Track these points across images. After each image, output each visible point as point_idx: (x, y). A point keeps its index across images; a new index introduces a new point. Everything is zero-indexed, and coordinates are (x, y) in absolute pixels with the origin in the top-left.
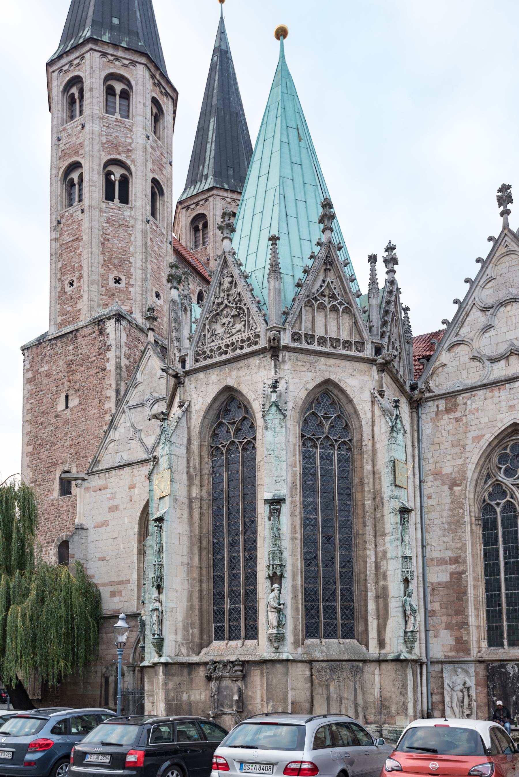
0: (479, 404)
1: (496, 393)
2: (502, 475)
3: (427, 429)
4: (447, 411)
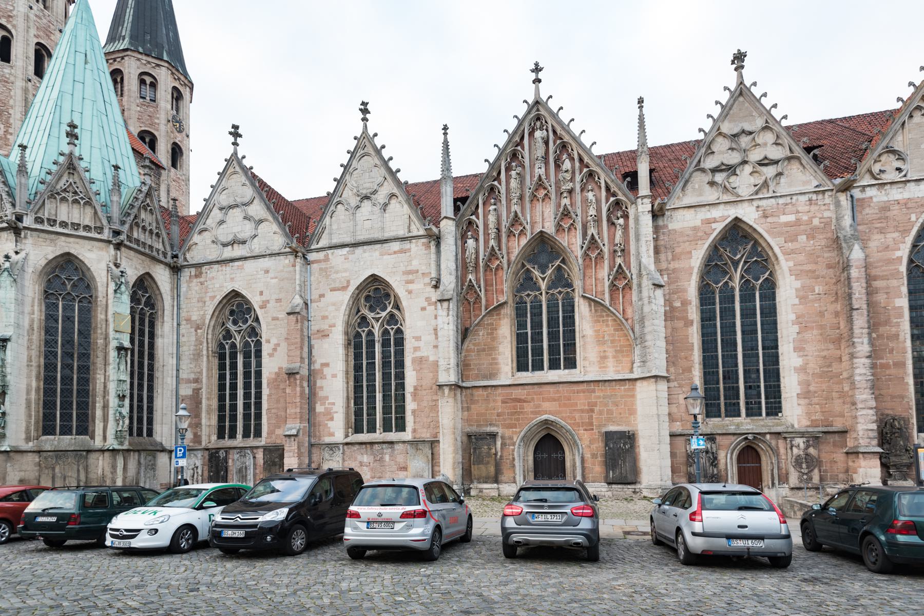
0: (214, 274)
1: (224, 268)
2: (230, 323)
3: (183, 289)
4: (196, 276)
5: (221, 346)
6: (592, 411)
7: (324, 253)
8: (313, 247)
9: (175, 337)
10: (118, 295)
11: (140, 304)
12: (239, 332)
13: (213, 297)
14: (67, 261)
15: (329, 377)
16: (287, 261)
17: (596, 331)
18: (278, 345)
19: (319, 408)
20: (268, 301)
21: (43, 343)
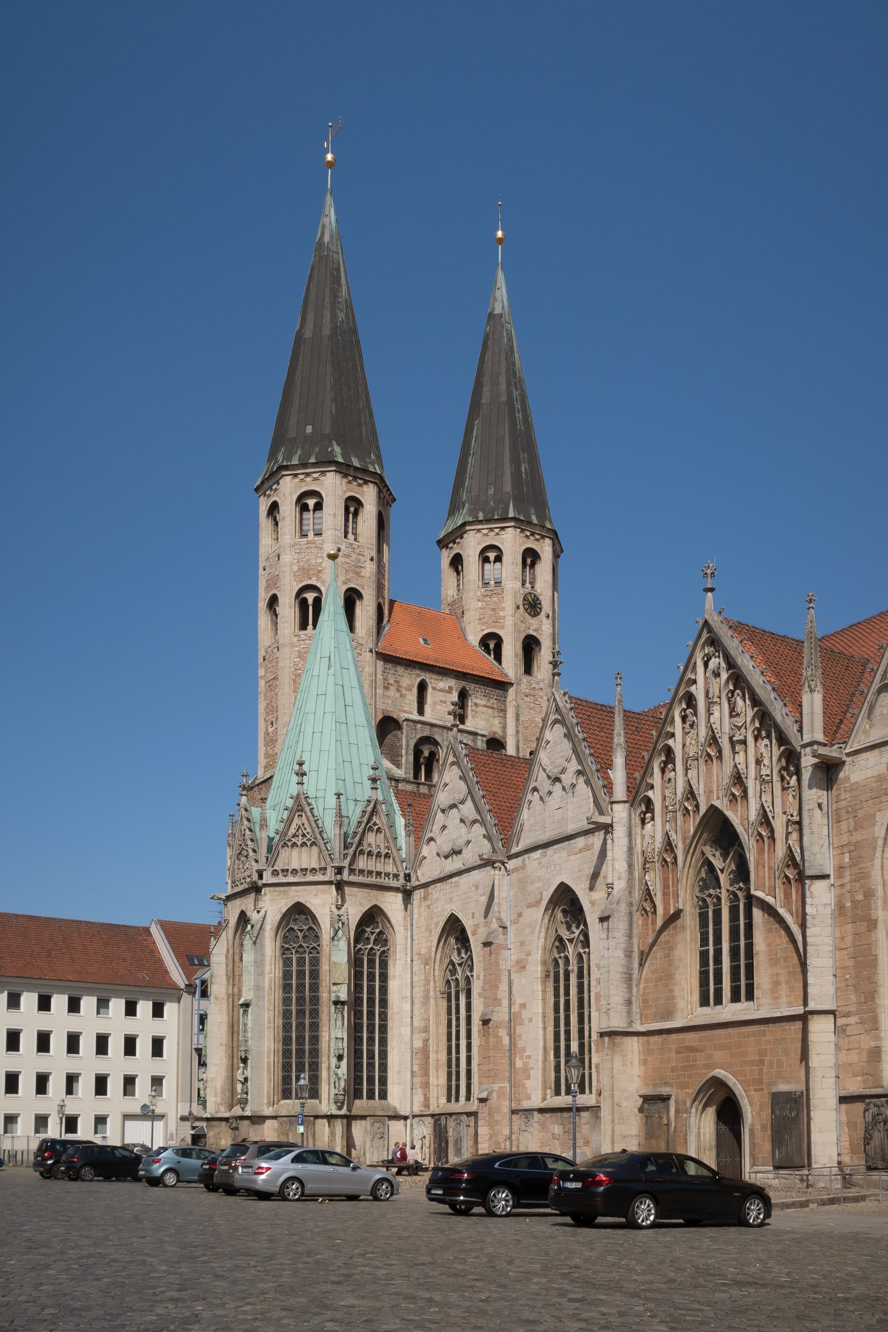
6: (762, 1062)
7: (520, 859)
9: (409, 976)
10: (336, 943)
11: (369, 944)
13: (437, 924)
14: (299, 910)
15: (526, 1022)
17: (769, 945)
19: (519, 1064)
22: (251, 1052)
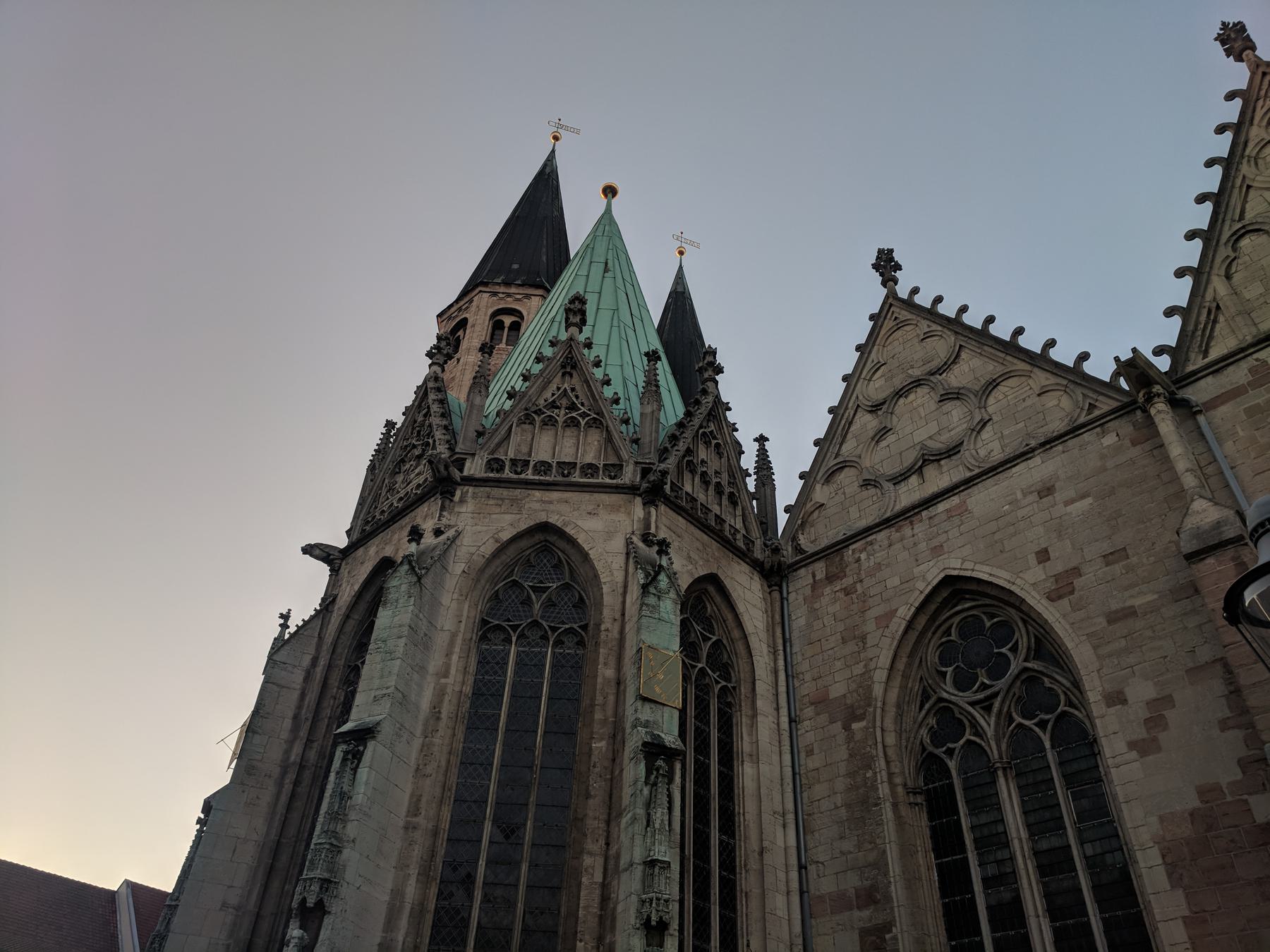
0: (880, 556)
1: (907, 531)
2: (949, 686)
3: (799, 620)
4: (830, 579)
5: (931, 766)
8: (1190, 368)
12: (985, 705)
16: (1110, 440)
18: (1166, 701)
20: (1076, 571)
21: (456, 761)
22: (344, 891)
